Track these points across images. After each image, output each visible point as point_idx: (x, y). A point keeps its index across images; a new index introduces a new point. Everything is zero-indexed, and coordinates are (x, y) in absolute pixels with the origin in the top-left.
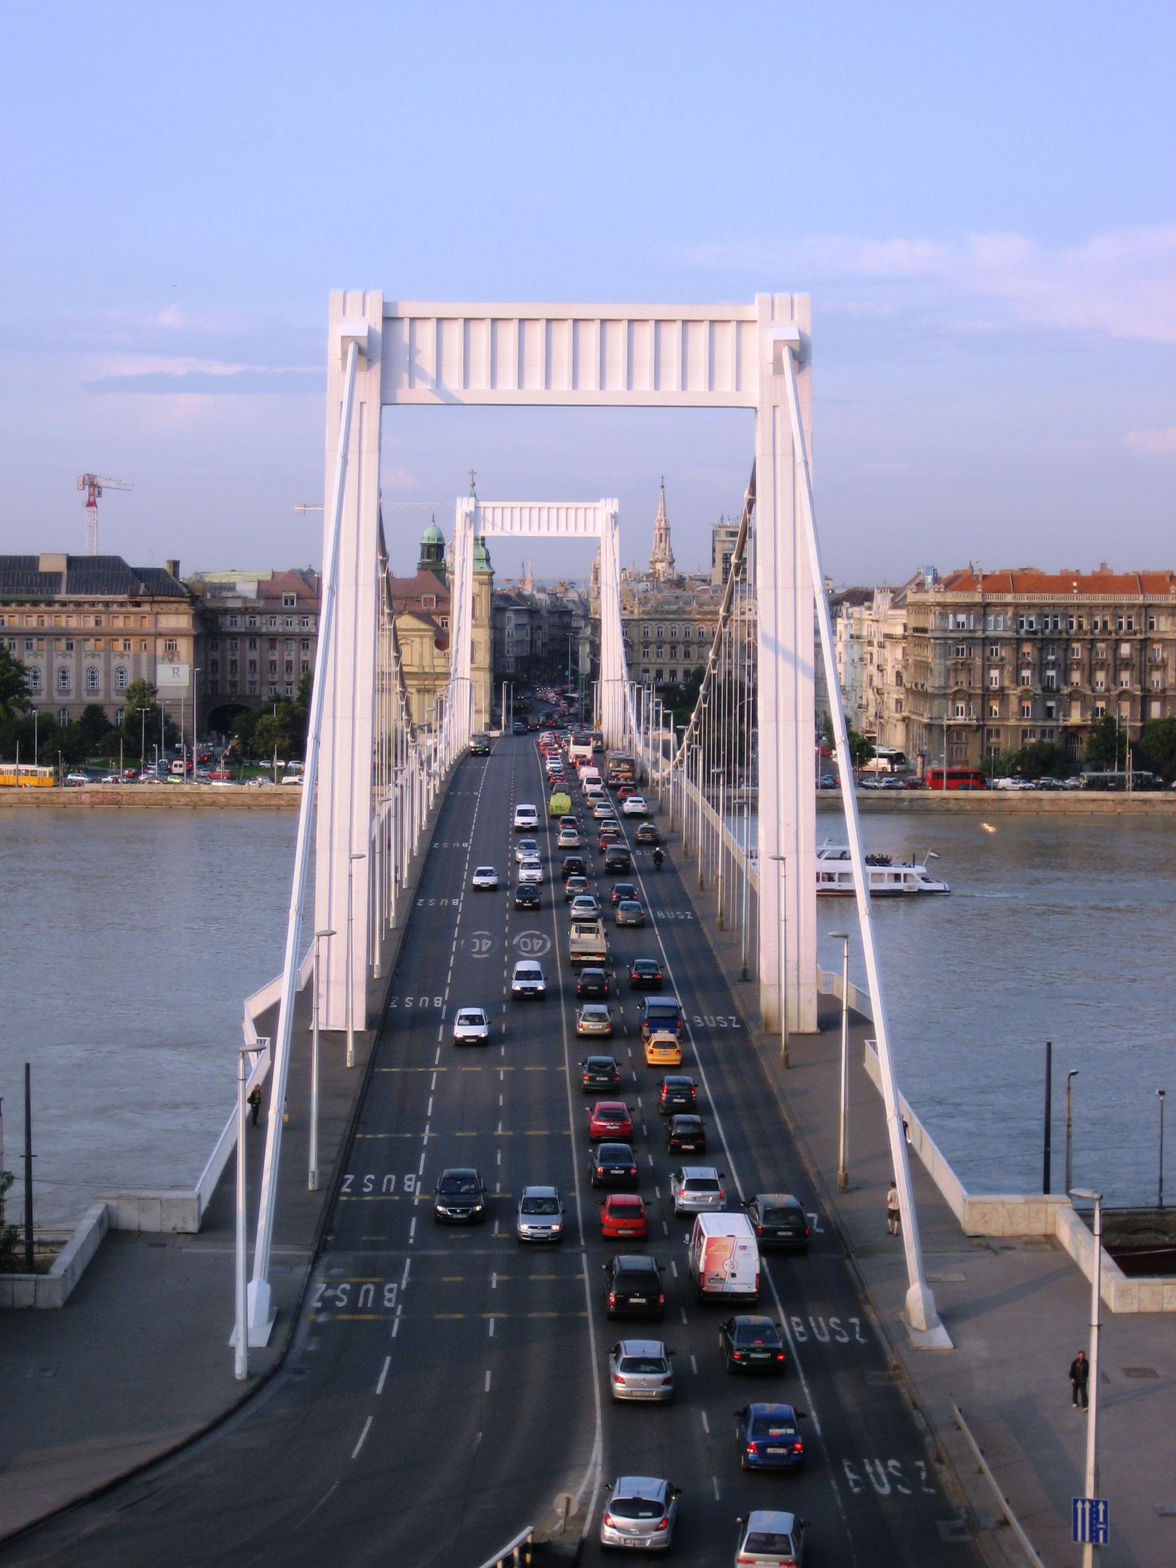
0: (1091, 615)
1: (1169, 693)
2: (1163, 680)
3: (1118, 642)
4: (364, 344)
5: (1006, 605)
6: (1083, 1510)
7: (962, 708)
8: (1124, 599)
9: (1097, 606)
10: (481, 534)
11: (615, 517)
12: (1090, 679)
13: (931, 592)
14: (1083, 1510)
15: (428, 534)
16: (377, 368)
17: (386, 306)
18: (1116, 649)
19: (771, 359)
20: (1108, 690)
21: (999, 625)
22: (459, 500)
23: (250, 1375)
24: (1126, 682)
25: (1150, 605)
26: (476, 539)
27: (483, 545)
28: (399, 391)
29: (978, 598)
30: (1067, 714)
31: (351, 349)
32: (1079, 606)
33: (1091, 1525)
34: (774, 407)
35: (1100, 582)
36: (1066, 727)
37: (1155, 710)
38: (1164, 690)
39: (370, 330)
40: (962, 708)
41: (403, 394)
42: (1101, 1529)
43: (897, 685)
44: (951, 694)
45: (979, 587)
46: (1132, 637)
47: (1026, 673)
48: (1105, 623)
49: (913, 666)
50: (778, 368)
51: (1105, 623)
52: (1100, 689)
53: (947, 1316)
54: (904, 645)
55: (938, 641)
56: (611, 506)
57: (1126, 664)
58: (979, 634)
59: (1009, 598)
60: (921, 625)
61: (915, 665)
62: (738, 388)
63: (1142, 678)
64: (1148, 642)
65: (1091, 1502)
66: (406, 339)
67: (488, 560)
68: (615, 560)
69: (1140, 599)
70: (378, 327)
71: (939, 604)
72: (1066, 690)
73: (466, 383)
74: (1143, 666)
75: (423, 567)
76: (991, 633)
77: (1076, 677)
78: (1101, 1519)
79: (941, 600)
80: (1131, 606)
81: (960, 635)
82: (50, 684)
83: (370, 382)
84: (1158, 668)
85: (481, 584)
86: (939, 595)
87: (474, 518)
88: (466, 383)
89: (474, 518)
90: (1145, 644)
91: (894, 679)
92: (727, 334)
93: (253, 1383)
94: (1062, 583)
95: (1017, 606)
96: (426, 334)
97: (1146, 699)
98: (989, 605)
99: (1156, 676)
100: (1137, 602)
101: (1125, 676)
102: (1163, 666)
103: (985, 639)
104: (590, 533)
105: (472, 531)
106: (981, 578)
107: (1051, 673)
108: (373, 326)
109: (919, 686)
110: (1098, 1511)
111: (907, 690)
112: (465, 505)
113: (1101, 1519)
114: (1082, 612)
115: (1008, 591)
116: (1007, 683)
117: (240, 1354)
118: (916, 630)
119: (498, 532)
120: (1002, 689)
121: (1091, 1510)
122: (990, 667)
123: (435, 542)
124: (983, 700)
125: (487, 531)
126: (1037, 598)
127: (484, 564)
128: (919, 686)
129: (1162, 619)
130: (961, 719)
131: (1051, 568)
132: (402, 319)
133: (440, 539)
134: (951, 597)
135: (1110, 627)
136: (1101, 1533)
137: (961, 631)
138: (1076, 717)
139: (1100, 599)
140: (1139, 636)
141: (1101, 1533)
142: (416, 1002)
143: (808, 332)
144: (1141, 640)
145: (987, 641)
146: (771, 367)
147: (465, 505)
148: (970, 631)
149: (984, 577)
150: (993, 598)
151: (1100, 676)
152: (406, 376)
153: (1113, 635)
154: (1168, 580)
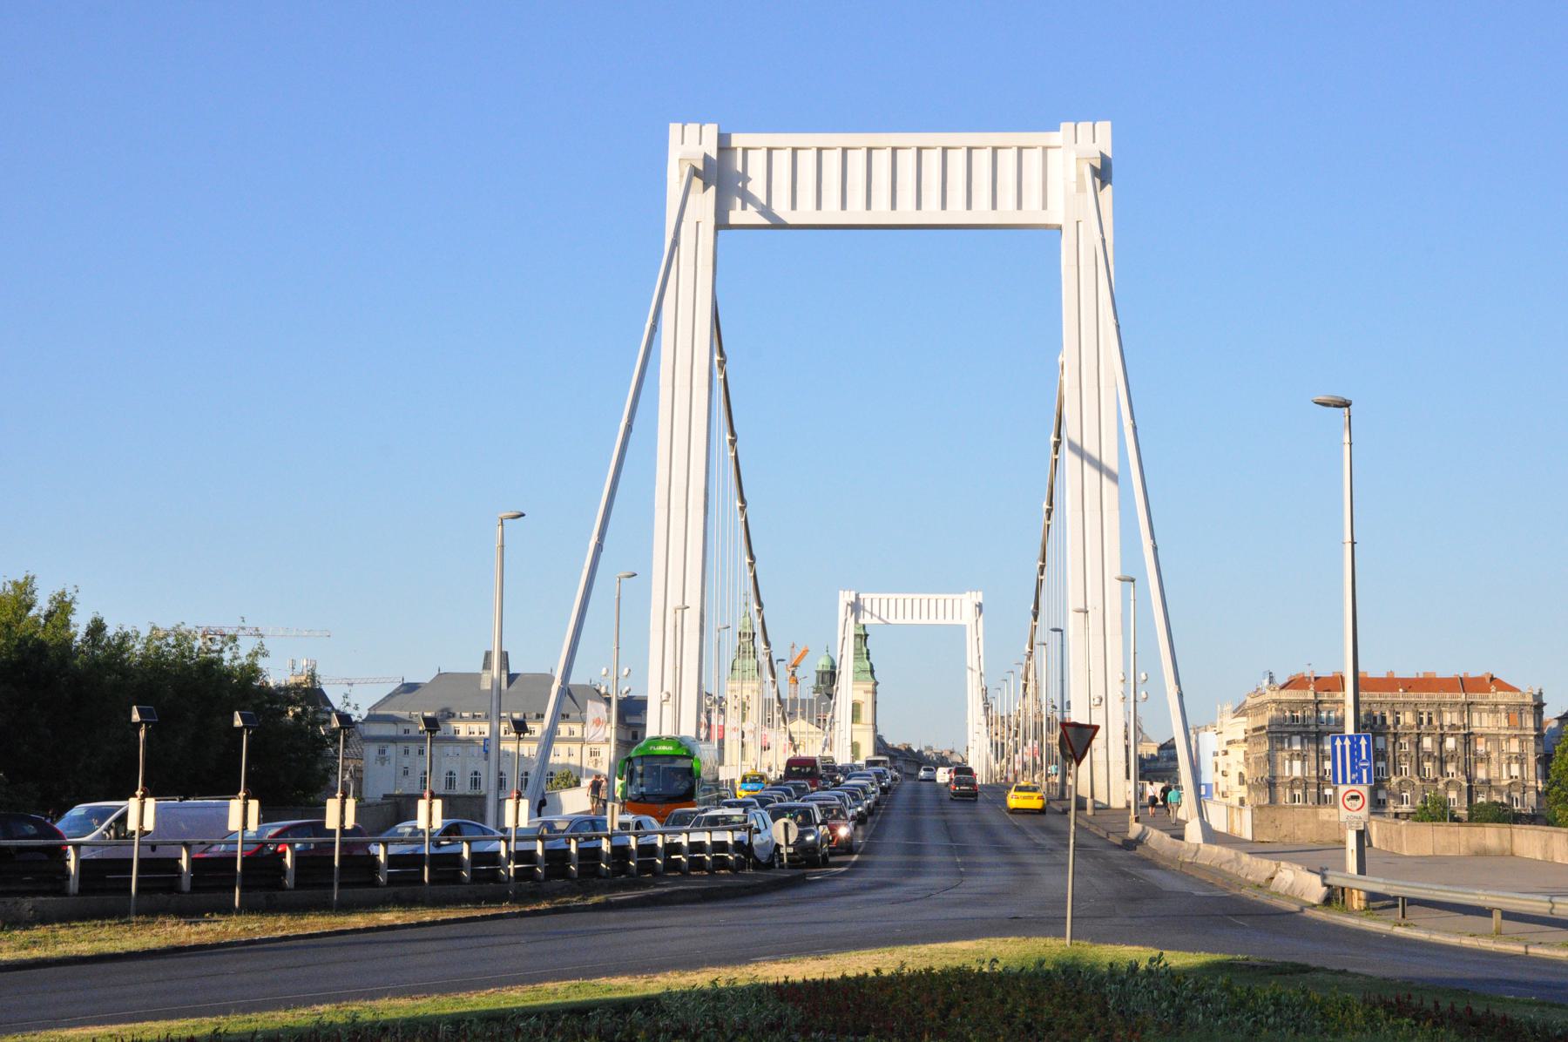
1: (1493, 784)
2: (1488, 773)
4: (700, 166)
6: (1343, 747)
7: (1299, 795)
10: (861, 621)
11: (980, 606)
13: (1268, 692)
14: (1343, 747)
15: (823, 663)
16: (712, 190)
18: (1442, 743)
19: (1073, 176)
22: (841, 592)
24: (1453, 774)
25: (1472, 703)
27: (868, 658)
28: (732, 213)
29: (1310, 696)
33: (1352, 765)
34: (1078, 222)
39: (706, 158)
40: (1299, 795)
41: (736, 216)
42: (1364, 767)
43: (1240, 784)
44: (1288, 783)
45: (1312, 687)
46: (1456, 732)
49: (1253, 764)
50: (1081, 188)
54: (1245, 749)
55: (1274, 735)
57: (1453, 756)
61: (1255, 763)
62: (1045, 207)
64: (1471, 737)
65: (1351, 737)
66: (739, 168)
67: (872, 672)
68: (979, 657)
69: (1462, 697)
70: (714, 155)
73: (794, 206)
74: (1469, 756)
78: (1364, 757)
79: (1278, 698)
80: (1456, 703)
86: (1274, 693)
87: (856, 607)
88: (794, 206)
89: (856, 607)
91: (1236, 780)
98: (1321, 702)
100: (1459, 699)
101: (1451, 768)
102: (1486, 759)
103: (1317, 733)
104: (957, 621)
105: (851, 620)
106: (1313, 680)
108: (708, 153)
109: (1259, 780)
110: (1360, 746)
111: (1250, 787)
113: (1364, 757)
118: (1255, 730)
119: (875, 621)
121: (1351, 747)
122: (1324, 758)
123: (829, 669)
124: (1318, 789)
125: (866, 619)
128: (1259, 780)
132: (736, 149)
133: (833, 667)
136: (1365, 771)
137: (1295, 726)
140: (1462, 731)
141: (1365, 771)
143: (1109, 154)
144: (1465, 735)
146: (1074, 186)
147: (847, 597)
148: (1304, 726)
149: (1316, 678)
152: (738, 201)
153: (1438, 729)
154: (1488, 681)
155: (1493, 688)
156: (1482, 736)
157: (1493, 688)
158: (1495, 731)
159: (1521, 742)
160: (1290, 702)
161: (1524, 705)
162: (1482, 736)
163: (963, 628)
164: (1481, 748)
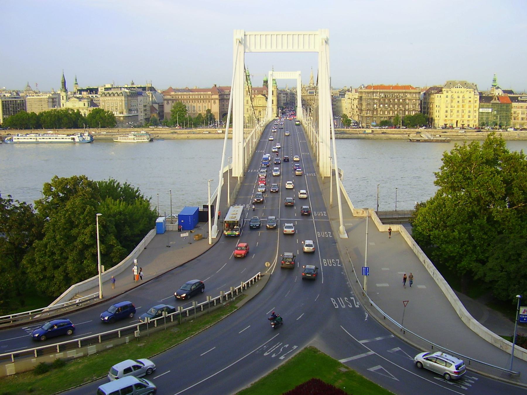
0: (394, 94)
2: (408, 107)
3: (400, 99)
5: (378, 92)
8: (401, 91)
9: (395, 92)
12: (394, 107)
17: (245, 33)
19: (321, 41)
20: (397, 109)
21: (375, 96)
23: (212, 243)
26: (273, 80)
29: (372, 91)
30: (389, 114)
31: (238, 41)
32: (392, 92)
35: (396, 87)
36: (389, 116)
37: (407, 113)
38: (408, 109)
47: (381, 106)
48: (397, 96)
50: (322, 44)
51: (397, 96)
52: (396, 109)
53: (348, 231)
56: (299, 72)
57: (401, 104)
58: (372, 98)
59: (378, 91)
60: (361, 96)
63: (404, 107)
67: (276, 83)
70: (243, 38)
71: (364, 92)
72: (389, 109)
74: (404, 104)
75: (264, 85)
76: (374, 98)
77: (391, 106)
80: (403, 92)
81: (369, 98)
82: (191, 110)
83: (242, 48)
84: (407, 105)
85: (275, 88)
87: (272, 75)
89: (272, 75)
90: (405, 99)
91: (356, 107)
92: (312, 37)
93: (213, 244)
94: (389, 87)
95: (380, 92)
96: (253, 38)
97: (405, 110)
99: (407, 106)
101: (401, 106)
102: (408, 104)
103: (373, 99)
104: (295, 78)
107: (386, 105)
112: (270, 72)
114: (393, 93)
115: (378, 89)
116: (378, 108)
117: (210, 239)
118: (360, 97)
120: (377, 109)
126: (384, 91)
127: (275, 84)
129: (408, 95)
130: (368, 115)
131: (386, 84)
134: (367, 90)
135: (398, 96)
138: (391, 114)
139: (396, 91)
140: (404, 98)
142: (253, 171)
143: (328, 38)
145: (374, 99)
150: (375, 91)
151: (396, 106)
155: (411, 89)
156: (408, 99)
157: (411, 89)
158: (410, 98)
159: (416, 100)
160: (368, 92)
161: (417, 92)
162: (408, 99)
163: (296, 79)
164: (407, 101)
